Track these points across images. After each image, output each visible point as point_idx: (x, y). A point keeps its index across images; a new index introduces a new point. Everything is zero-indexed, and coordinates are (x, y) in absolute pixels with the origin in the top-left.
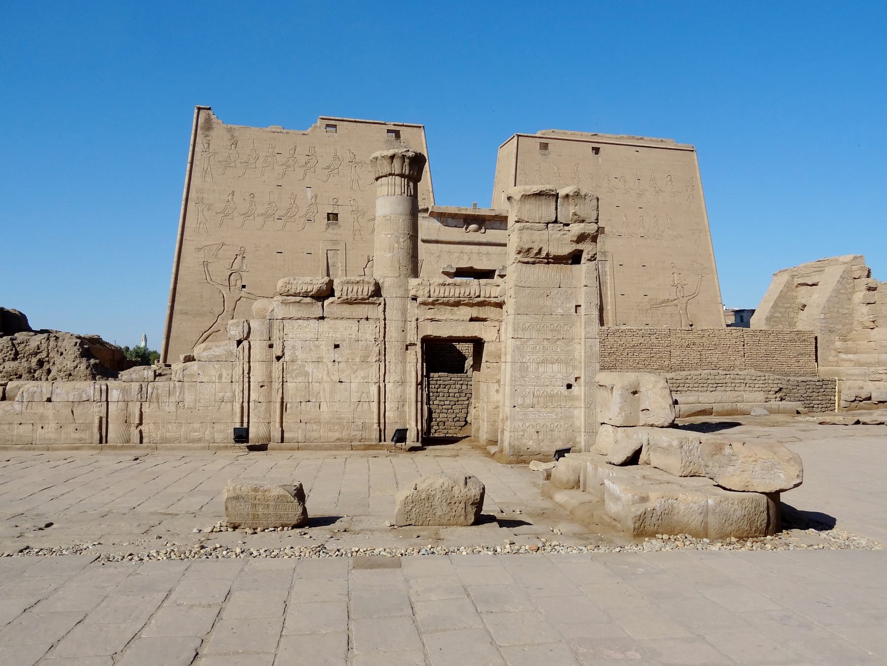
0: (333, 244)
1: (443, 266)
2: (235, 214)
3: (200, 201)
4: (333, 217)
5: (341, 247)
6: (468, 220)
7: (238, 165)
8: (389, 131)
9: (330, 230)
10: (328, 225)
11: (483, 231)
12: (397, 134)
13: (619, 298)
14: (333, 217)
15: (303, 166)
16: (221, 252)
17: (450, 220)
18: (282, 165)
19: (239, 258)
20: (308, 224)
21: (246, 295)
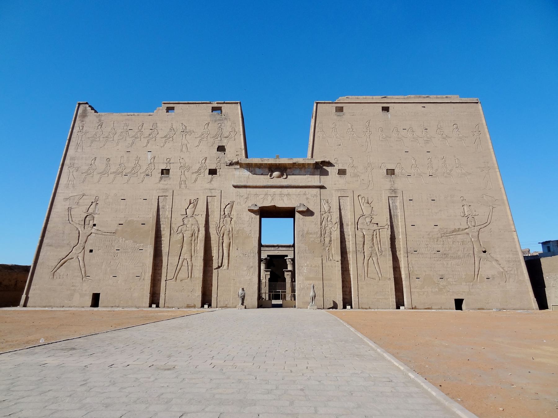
0: (164, 192)
1: (250, 204)
2: (95, 173)
3: (72, 165)
4: (165, 172)
5: (169, 194)
6: (271, 168)
7: (101, 139)
8: (214, 109)
9: (162, 182)
10: (161, 178)
11: (285, 176)
12: (219, 109)
13: (410, 228)
14: (165, 172)
15: (147, 137)
16: (81, 201)
17: (257, 170)
18: (132, 137)
19: (94, 204)
20: (147, 177)
21: (95, 232)
